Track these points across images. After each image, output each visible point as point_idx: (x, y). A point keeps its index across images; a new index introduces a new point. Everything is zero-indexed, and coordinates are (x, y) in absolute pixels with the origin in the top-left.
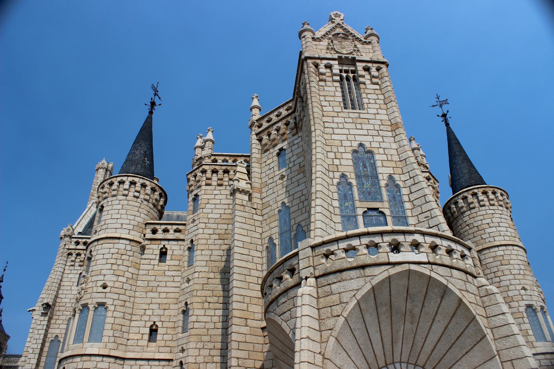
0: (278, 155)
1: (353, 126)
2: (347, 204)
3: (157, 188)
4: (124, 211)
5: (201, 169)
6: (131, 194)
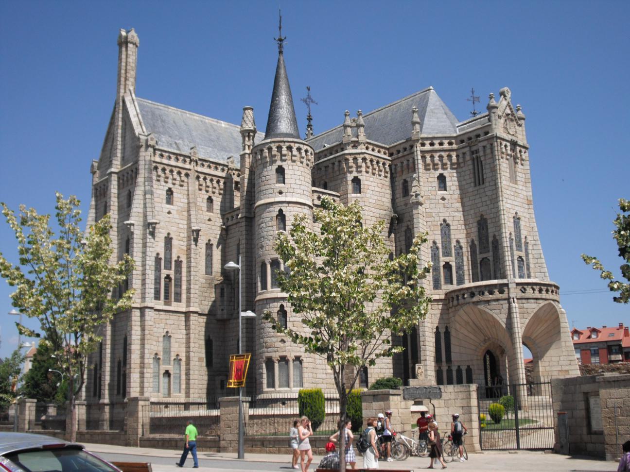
0: (438, 178)
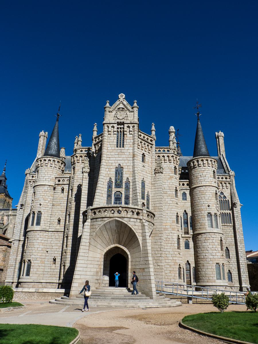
1: (118, 156)
2: (110, 190)
3: (60, 161)
4: (46, 173)
5: (75, 156)
6: (49, 165)
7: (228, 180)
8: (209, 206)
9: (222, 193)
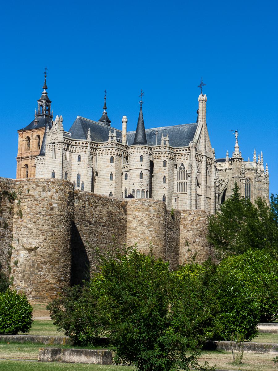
1: (52, 165)
4: (40, 169)
7: (187, 152)
8: (134, 185)
9: (182, 165)
